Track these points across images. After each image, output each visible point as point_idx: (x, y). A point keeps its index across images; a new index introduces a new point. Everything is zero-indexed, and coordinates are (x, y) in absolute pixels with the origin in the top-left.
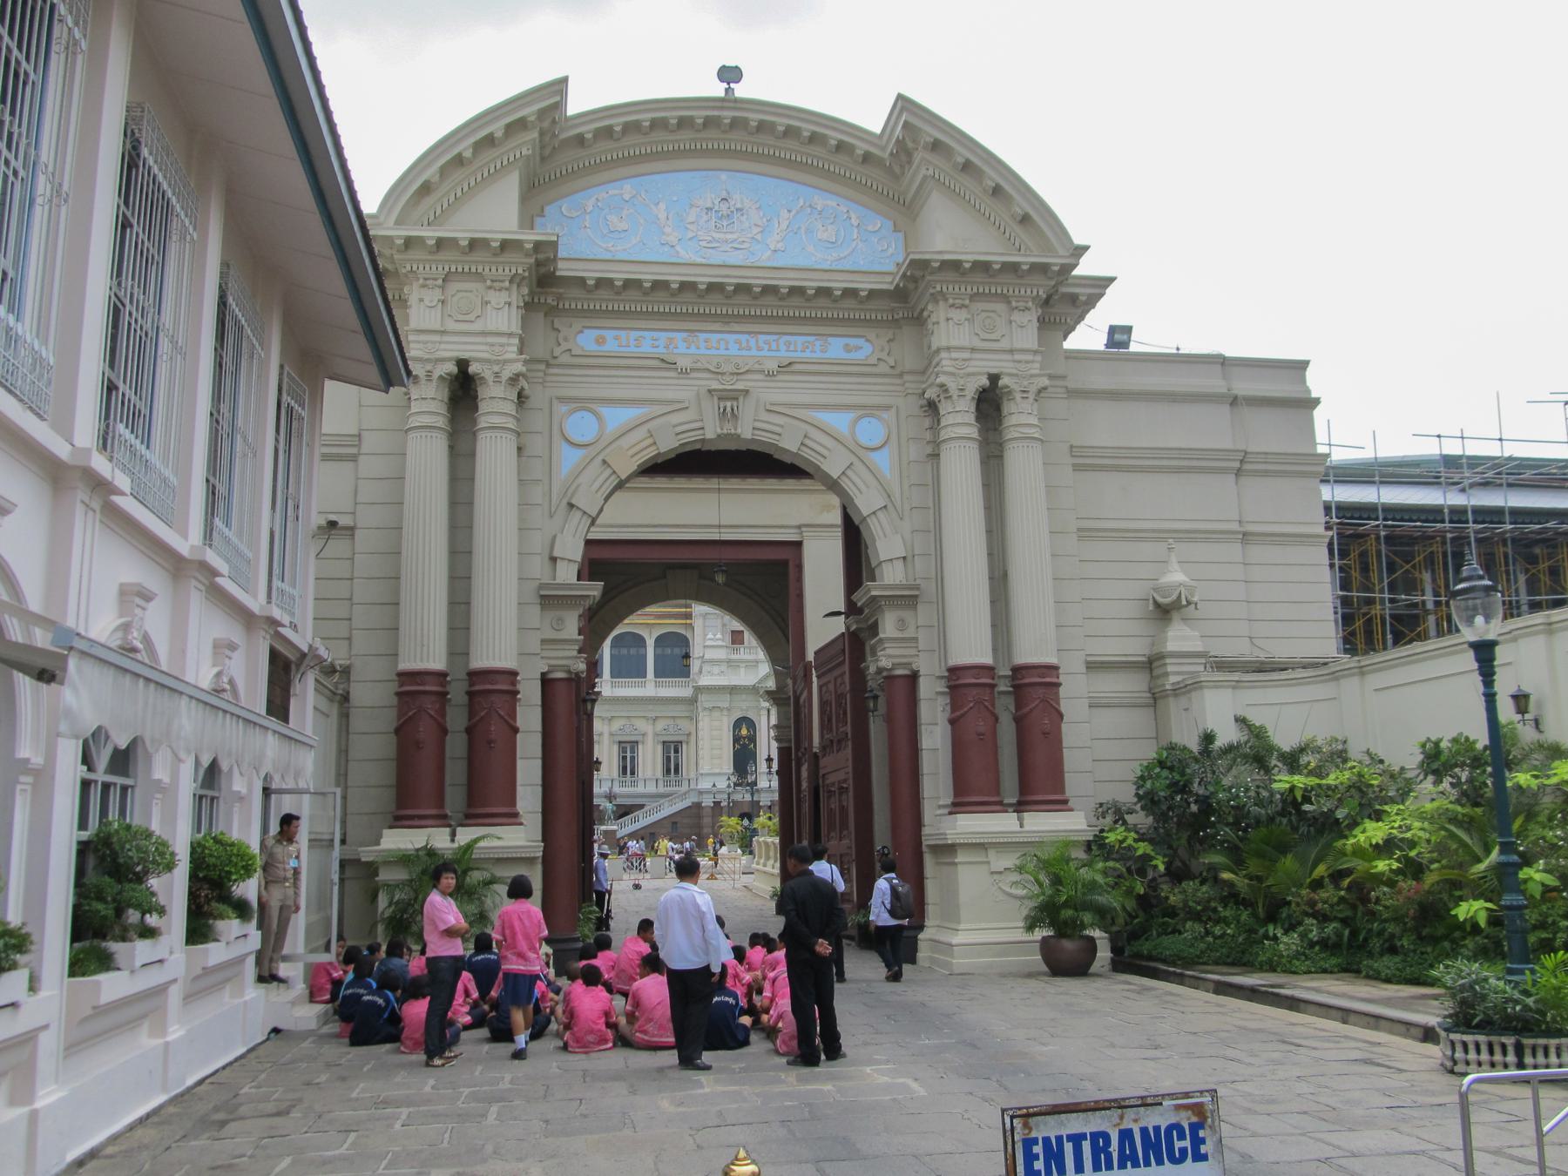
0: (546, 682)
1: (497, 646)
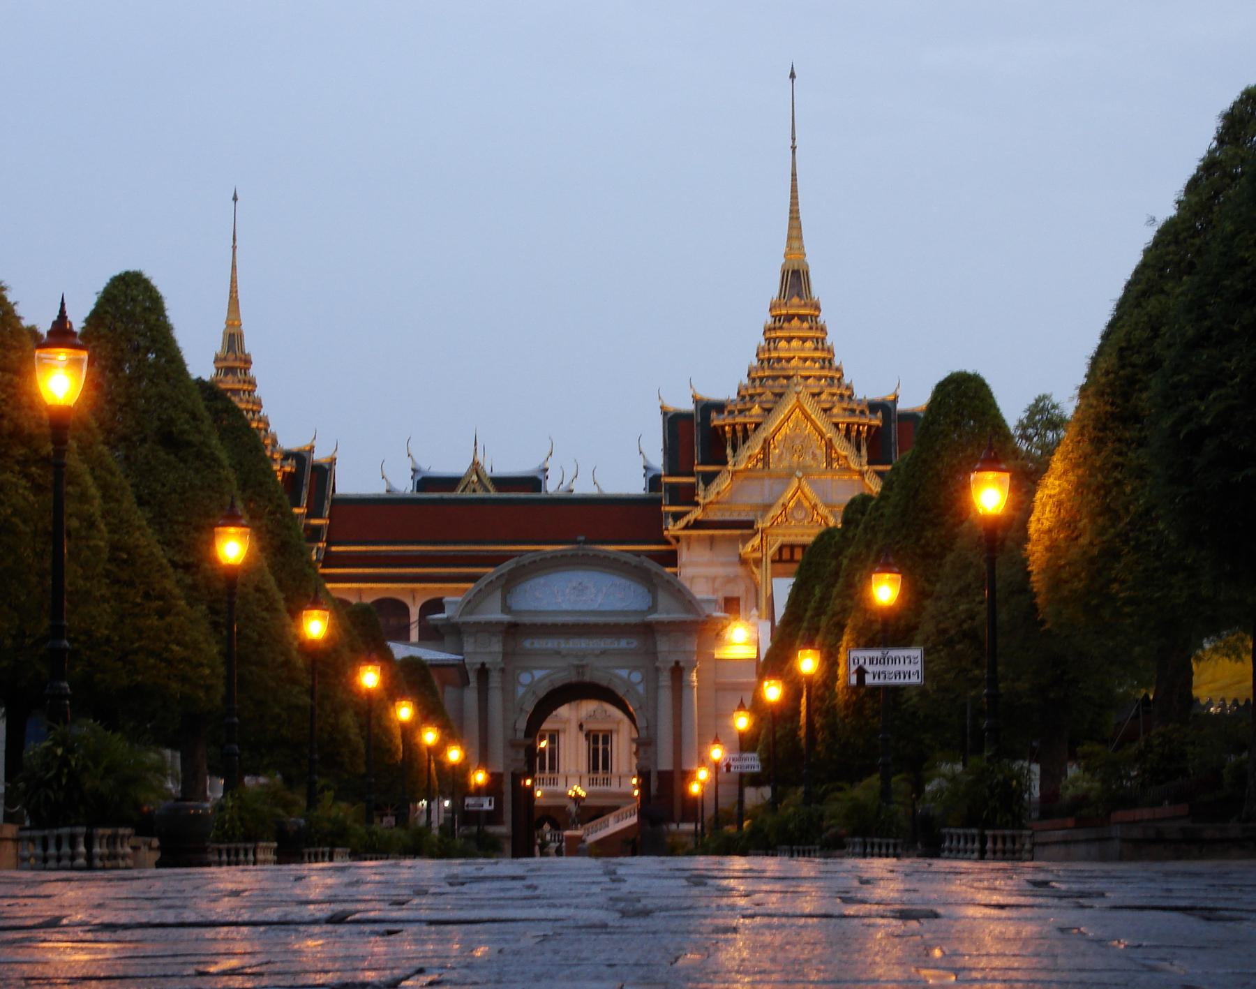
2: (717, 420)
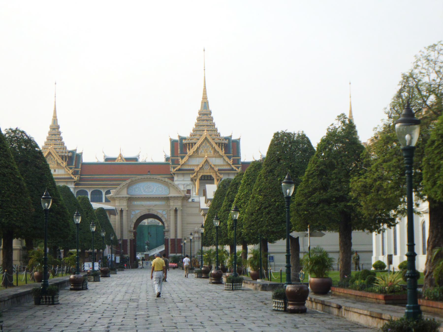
0: (130, 240)
1: (125, 238)
2: (184, 141)
